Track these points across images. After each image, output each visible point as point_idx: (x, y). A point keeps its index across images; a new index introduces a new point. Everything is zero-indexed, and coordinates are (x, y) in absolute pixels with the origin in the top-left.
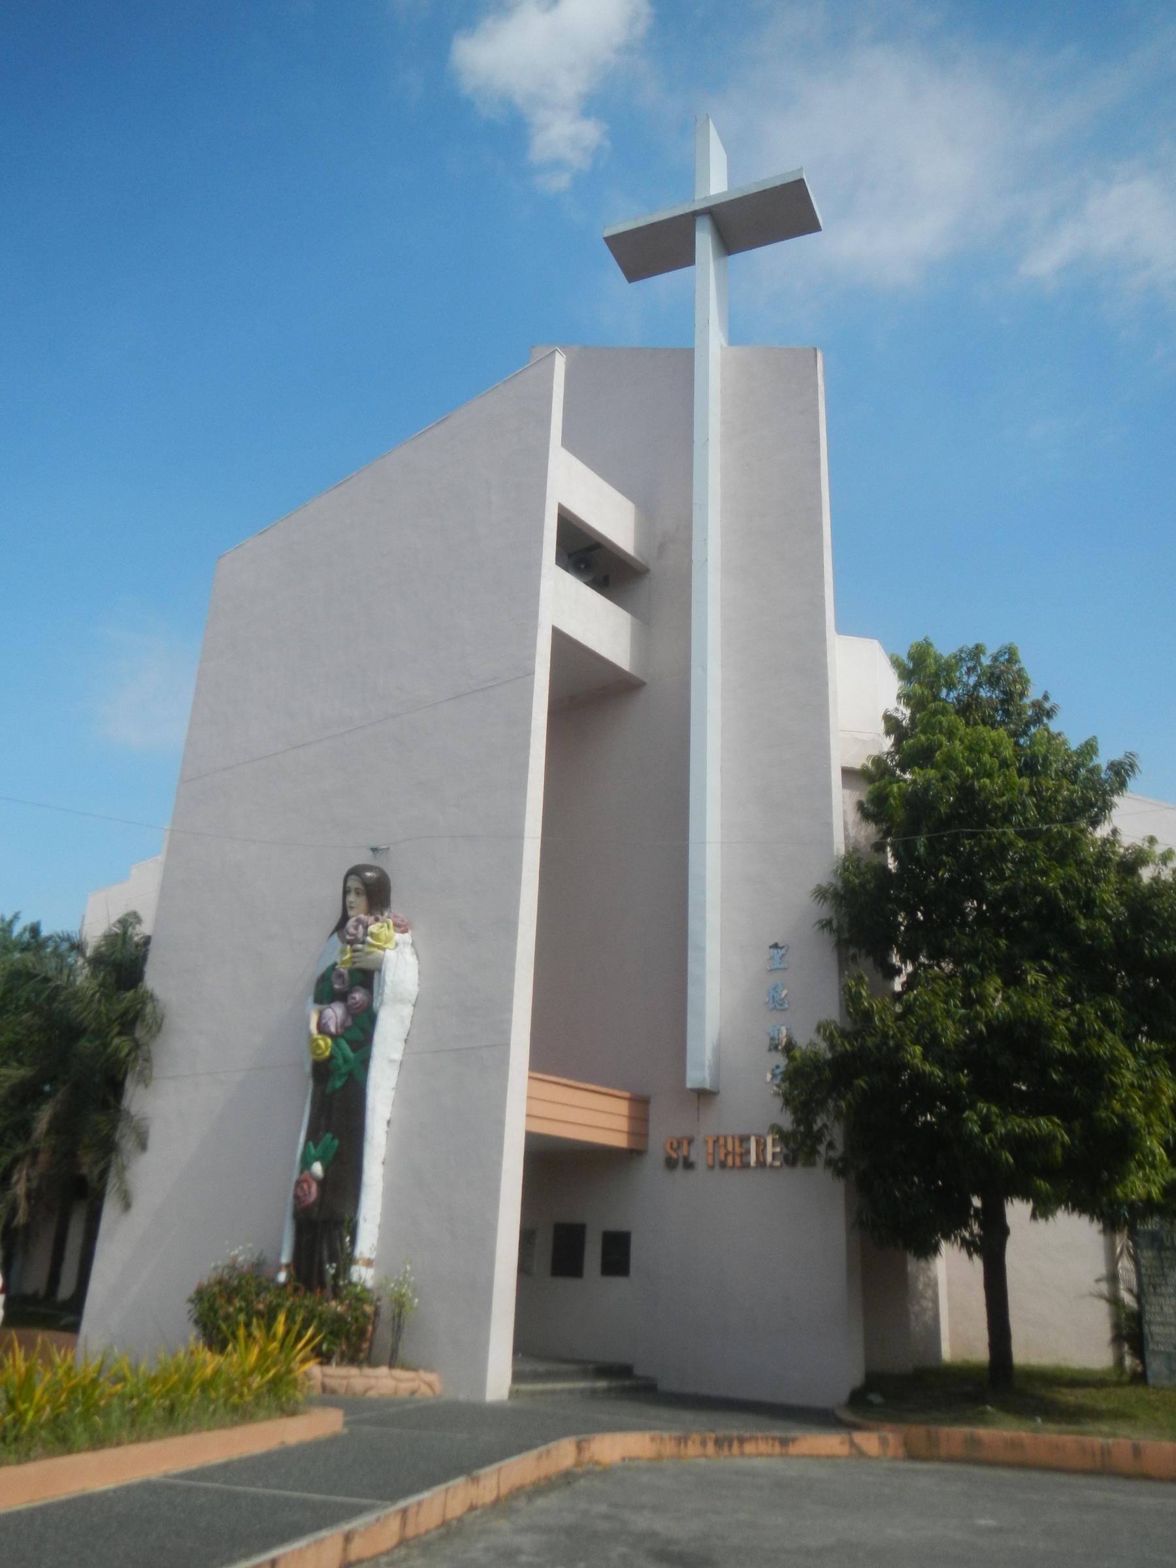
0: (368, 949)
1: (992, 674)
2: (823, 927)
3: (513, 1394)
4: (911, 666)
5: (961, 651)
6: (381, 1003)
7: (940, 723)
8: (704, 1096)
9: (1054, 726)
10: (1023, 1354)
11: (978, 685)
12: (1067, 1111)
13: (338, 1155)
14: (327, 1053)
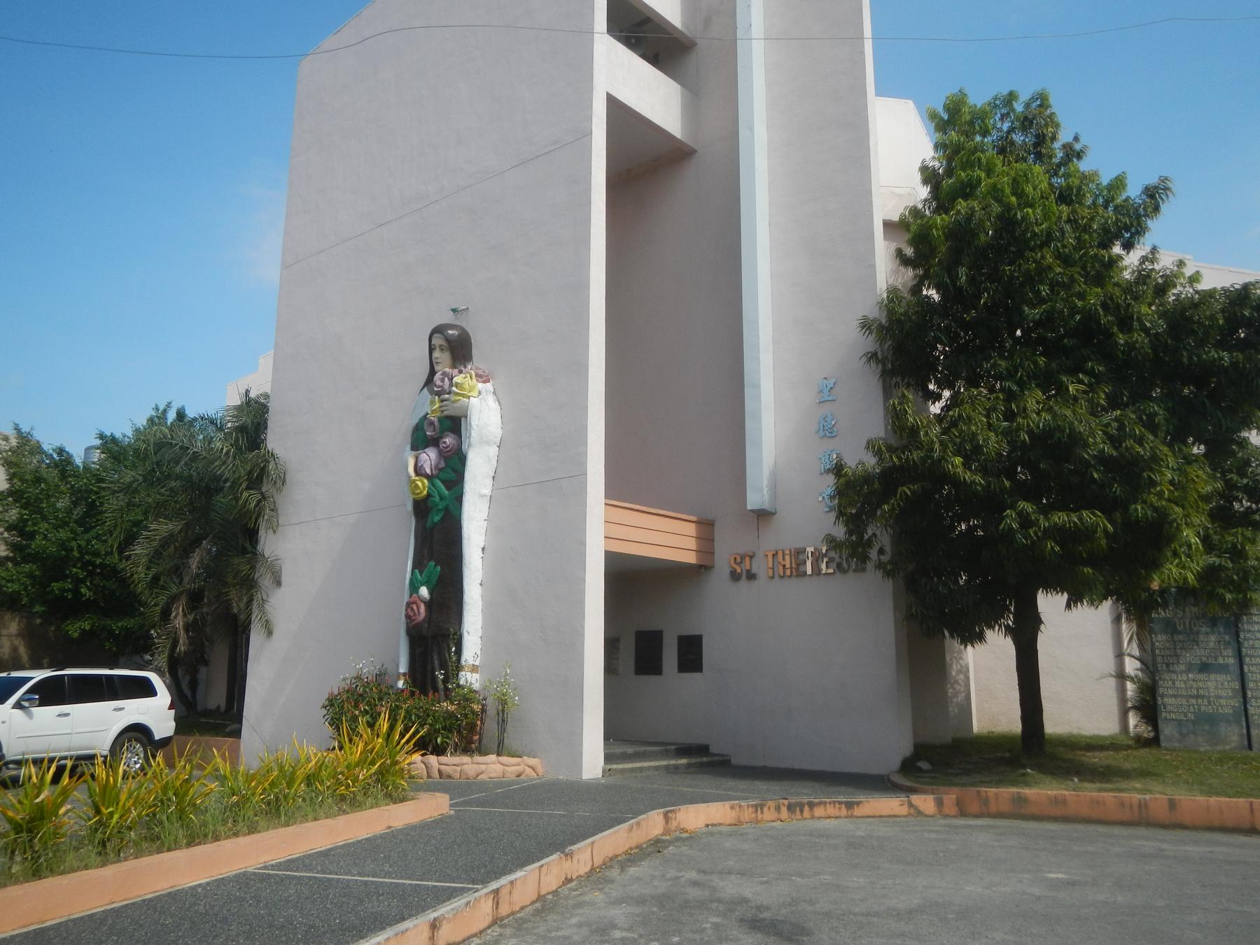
0: (453, 398)
1: (1026, 118)
2: (869, 360)
3: (606, 772)
4: (946, 117)
5: (995, 98)
6: (469, 446)
7: (979, 159)
8: (763, 516)
9: (1084, 166)
10: (1056, 722)
11: (1011, 130)
12: (1108, 507)
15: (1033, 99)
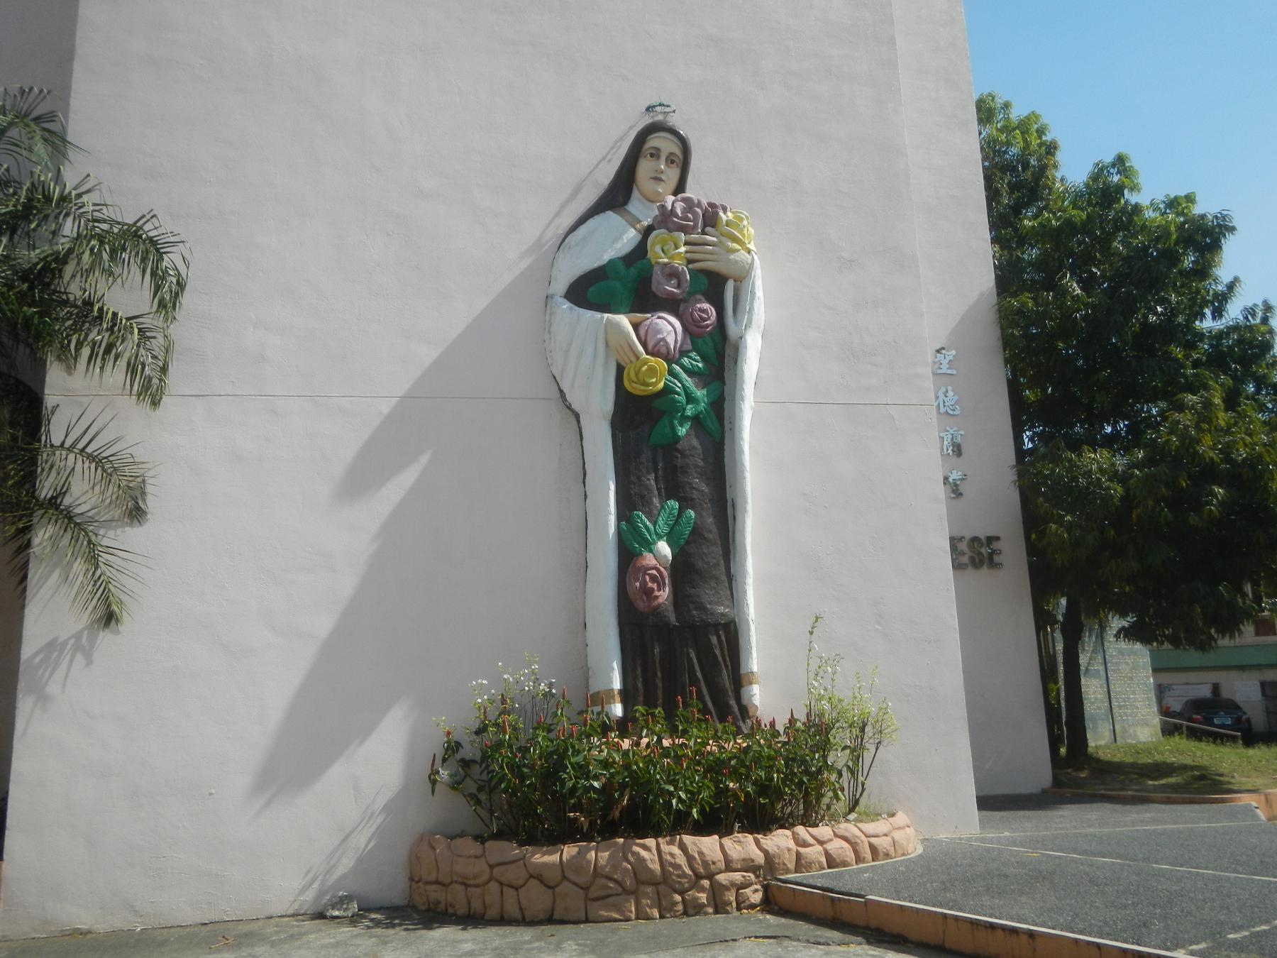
13: (696, 532)
14: (661, 385)
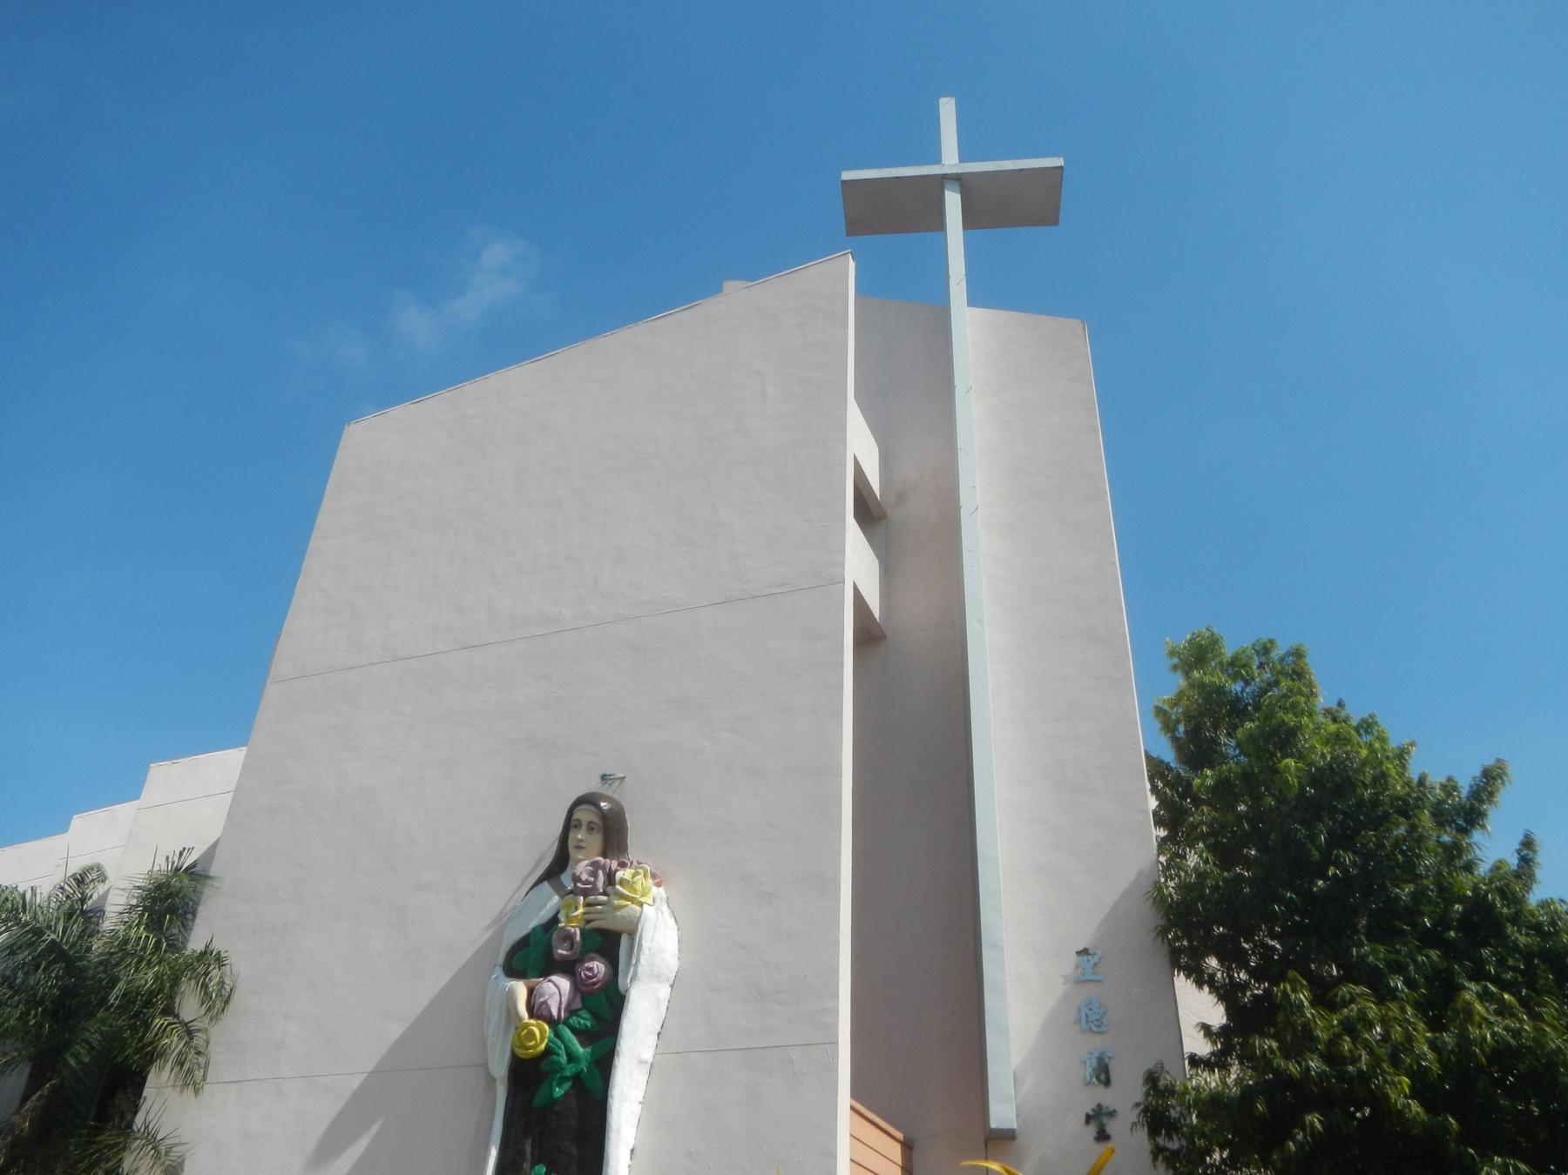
14: (543, 1047)
15: (1289, 654)
